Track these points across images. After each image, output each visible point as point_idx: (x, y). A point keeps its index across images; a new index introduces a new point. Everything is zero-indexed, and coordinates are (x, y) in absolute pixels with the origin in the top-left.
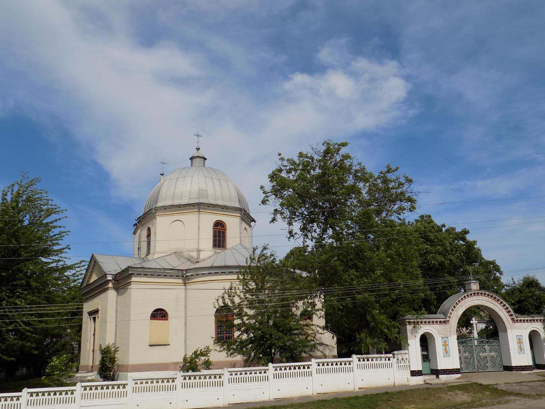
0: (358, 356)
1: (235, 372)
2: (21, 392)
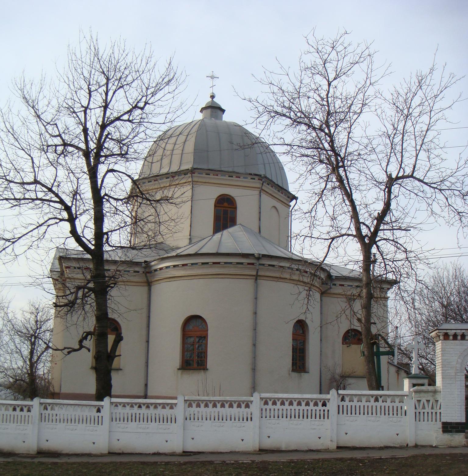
0: (42, 400)
1: (357, 397)
2: (103, 401)
